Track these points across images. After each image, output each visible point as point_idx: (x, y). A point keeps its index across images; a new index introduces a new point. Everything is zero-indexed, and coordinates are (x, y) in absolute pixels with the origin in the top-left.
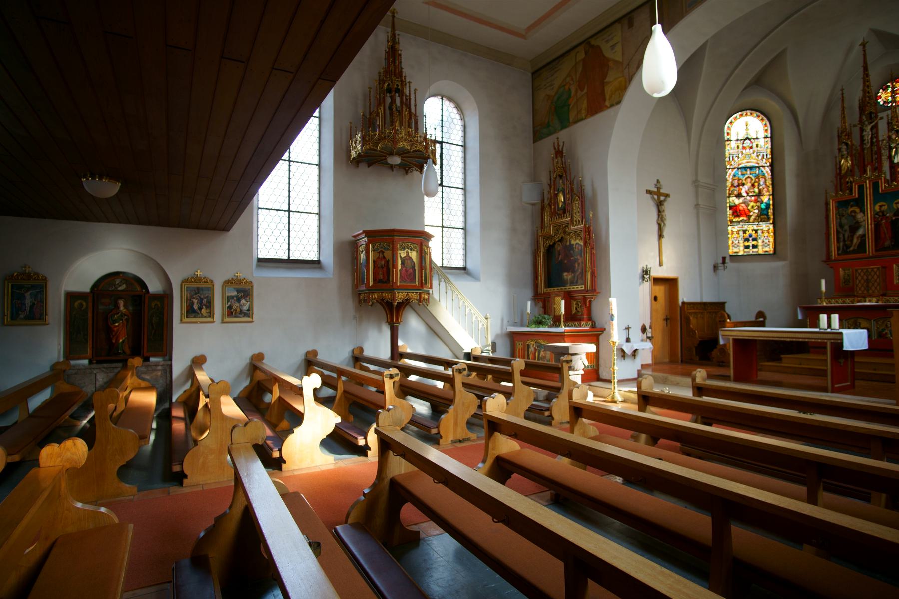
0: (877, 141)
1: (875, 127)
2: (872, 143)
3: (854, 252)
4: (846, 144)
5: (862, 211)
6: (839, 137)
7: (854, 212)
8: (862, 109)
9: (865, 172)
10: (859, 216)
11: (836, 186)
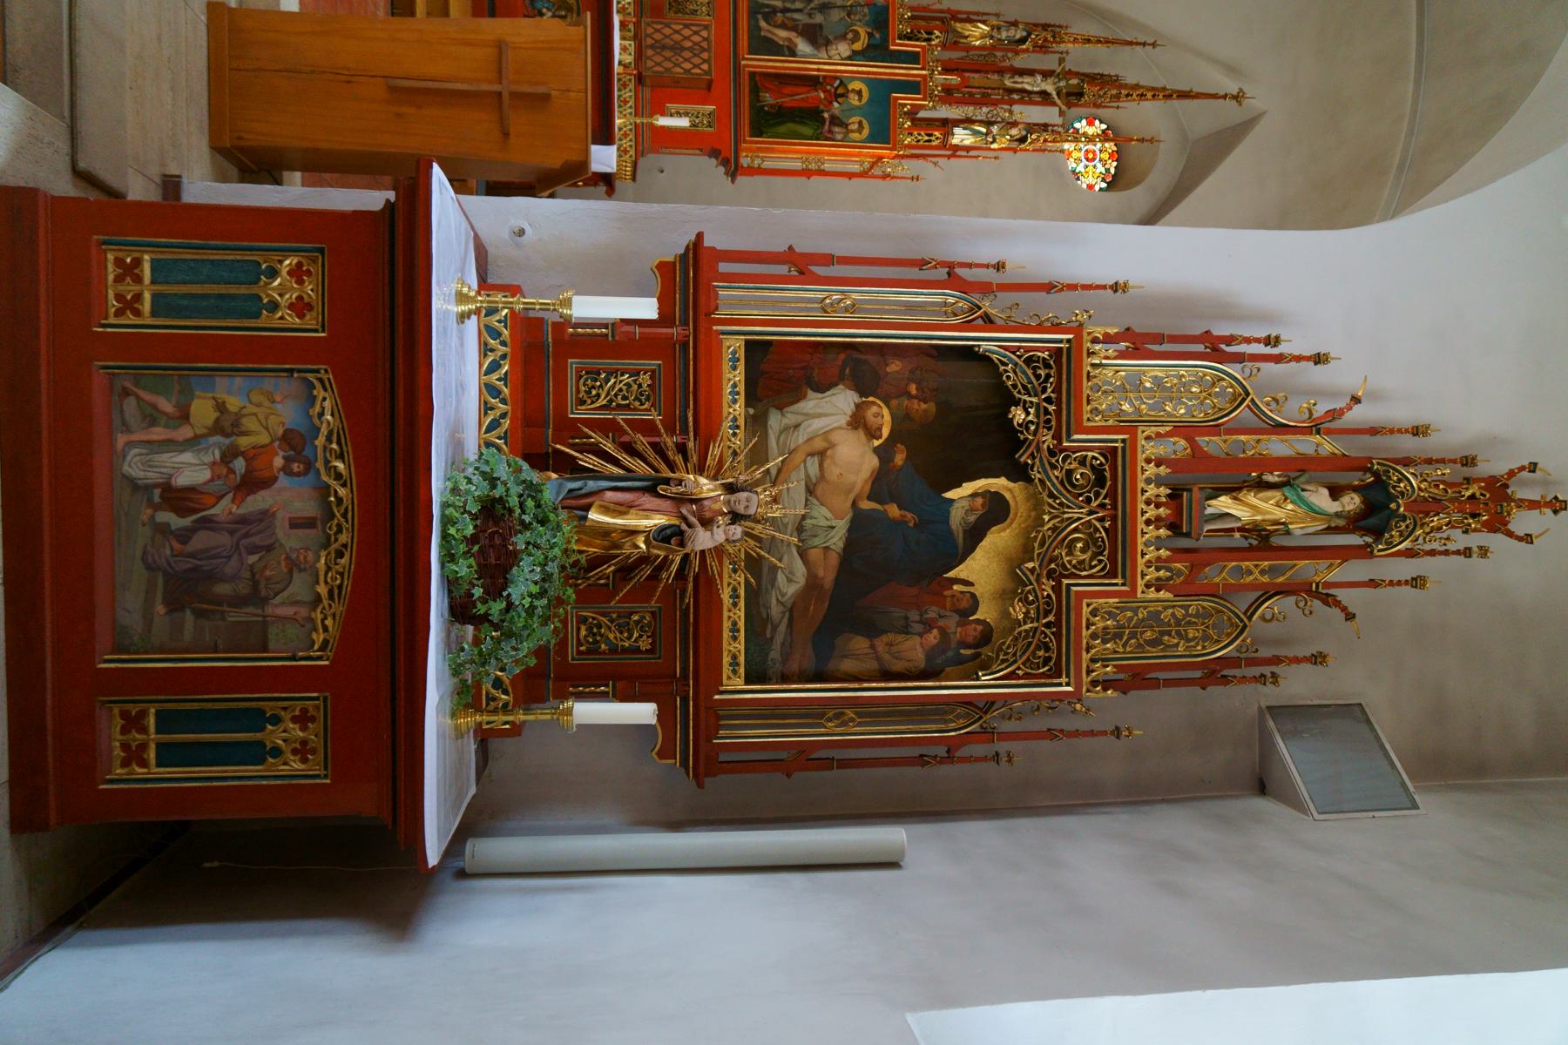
0: (1012, 103)
2: (1011, 91)
3: (754, 29)
4: (1023, 40)
5: (855, 55)
6: (1045, 27)
7: (856, 37)
8: (1093, 78)
9: (947, 70)
10: (843, 49)
11: (925, 9)
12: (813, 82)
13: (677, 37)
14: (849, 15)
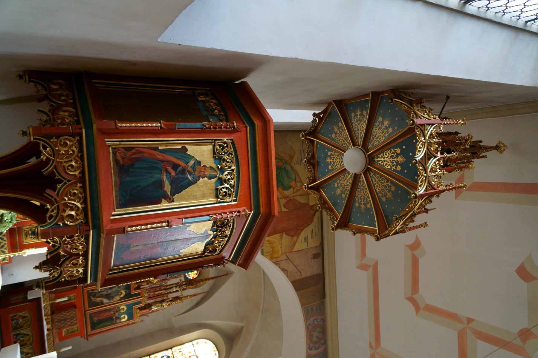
1: (177, 291)
10: (118, 298)
12: (110, 310)
13: (65, 316)
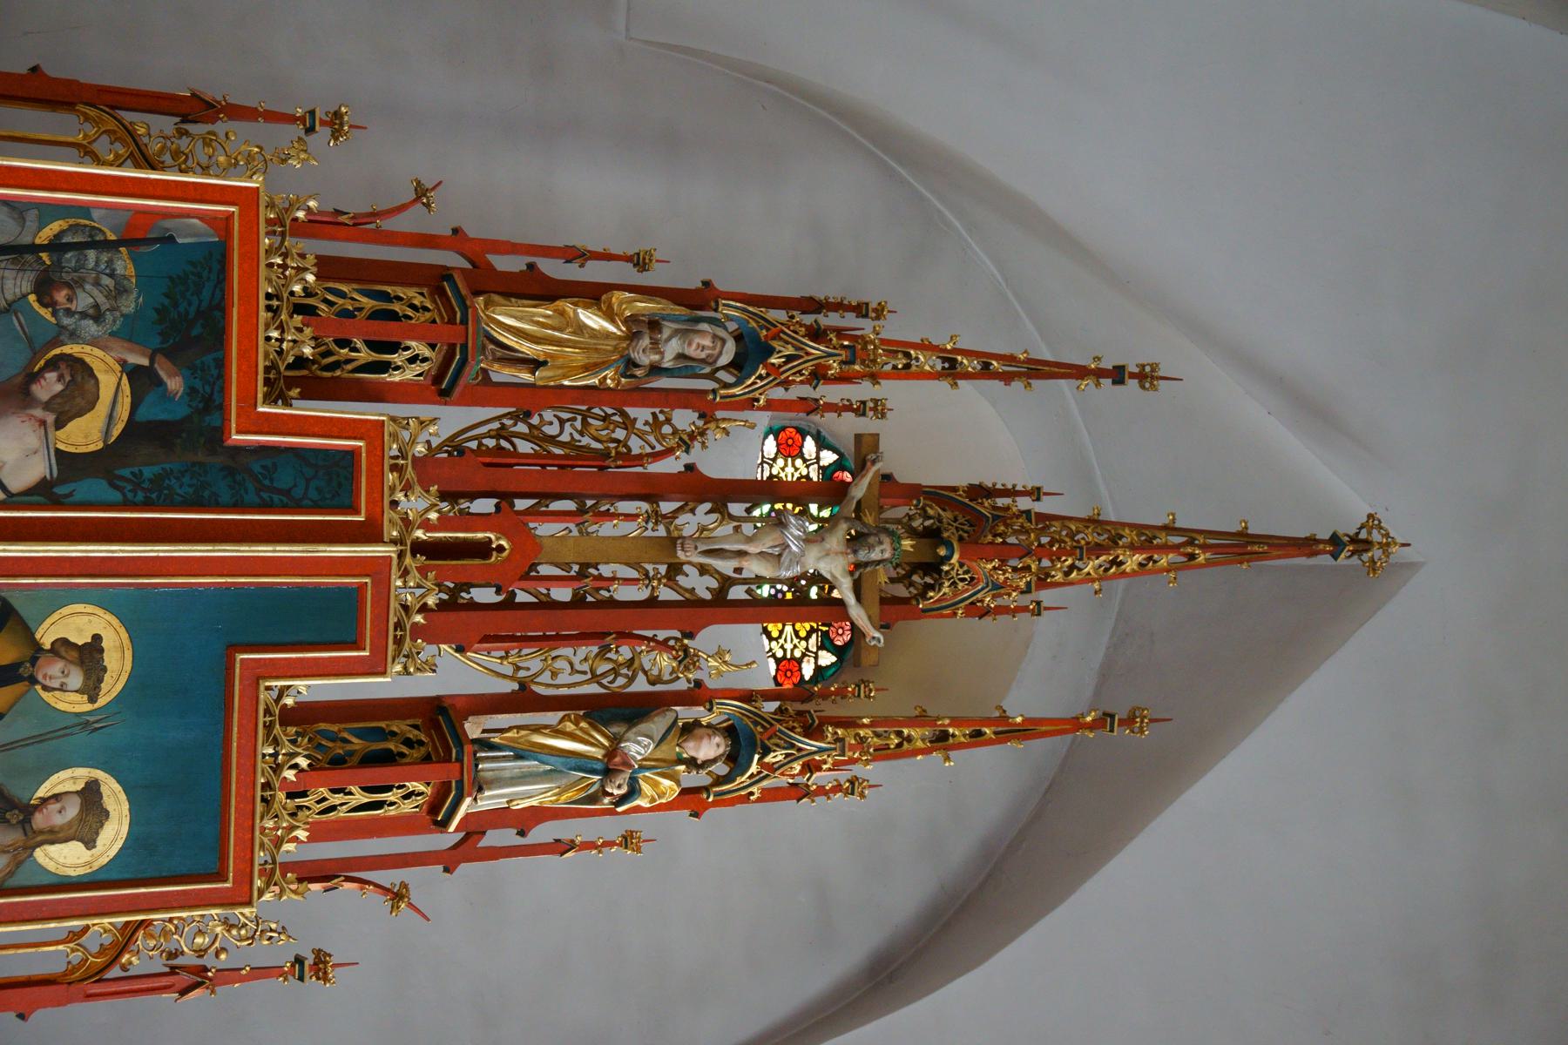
11: (359, 226)
14: (44, 288)
